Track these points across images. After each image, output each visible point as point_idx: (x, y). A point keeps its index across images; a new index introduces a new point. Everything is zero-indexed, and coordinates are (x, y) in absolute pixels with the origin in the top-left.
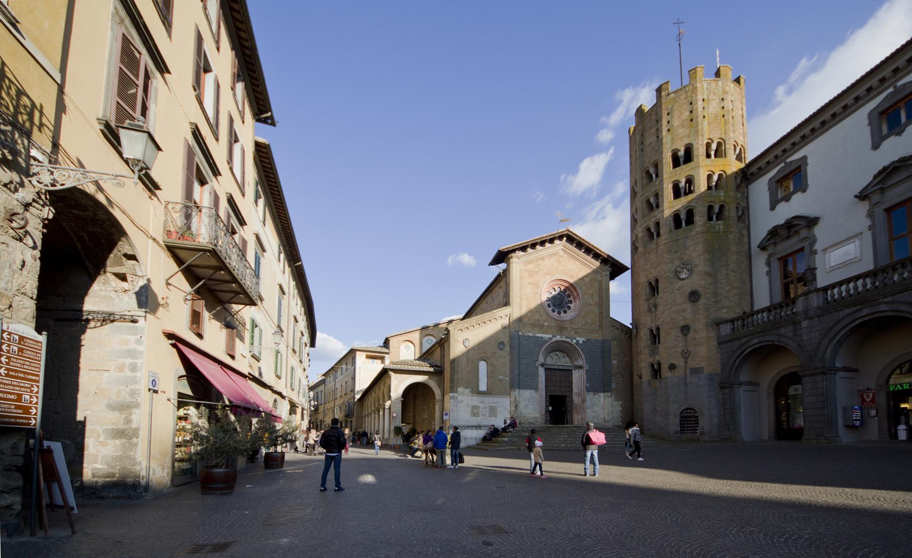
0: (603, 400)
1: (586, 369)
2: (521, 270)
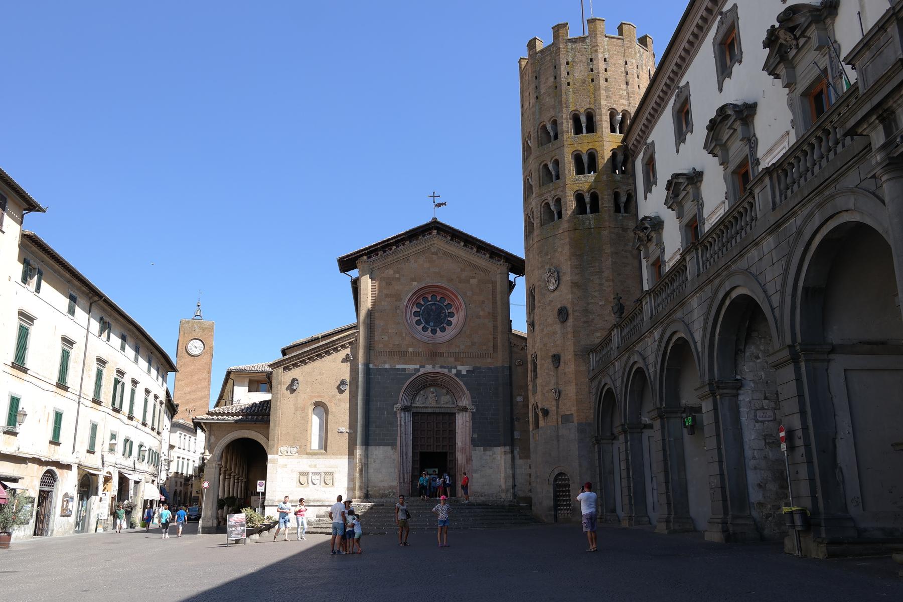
0: (499, 456)
1: (473, 413)
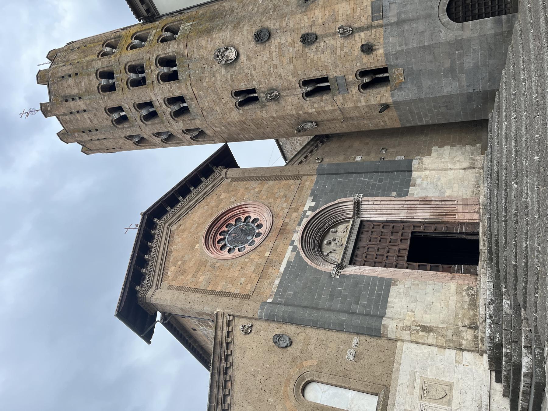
0: (427, 173)
1: (363, 196)
2: (170, 287)
